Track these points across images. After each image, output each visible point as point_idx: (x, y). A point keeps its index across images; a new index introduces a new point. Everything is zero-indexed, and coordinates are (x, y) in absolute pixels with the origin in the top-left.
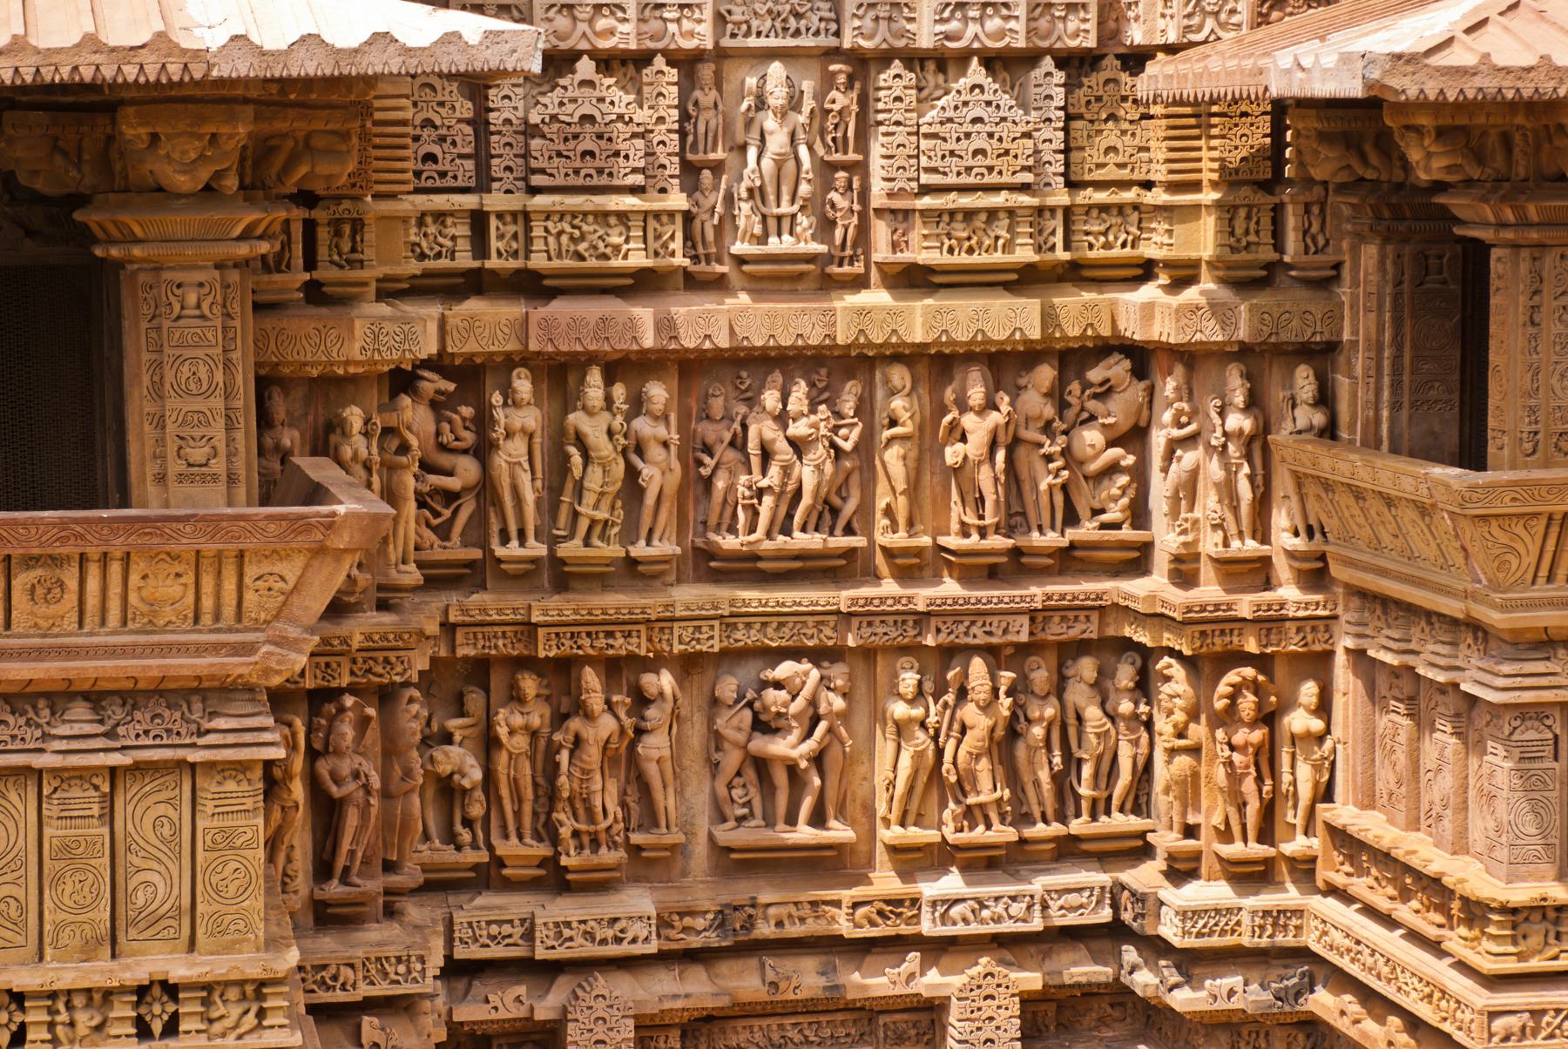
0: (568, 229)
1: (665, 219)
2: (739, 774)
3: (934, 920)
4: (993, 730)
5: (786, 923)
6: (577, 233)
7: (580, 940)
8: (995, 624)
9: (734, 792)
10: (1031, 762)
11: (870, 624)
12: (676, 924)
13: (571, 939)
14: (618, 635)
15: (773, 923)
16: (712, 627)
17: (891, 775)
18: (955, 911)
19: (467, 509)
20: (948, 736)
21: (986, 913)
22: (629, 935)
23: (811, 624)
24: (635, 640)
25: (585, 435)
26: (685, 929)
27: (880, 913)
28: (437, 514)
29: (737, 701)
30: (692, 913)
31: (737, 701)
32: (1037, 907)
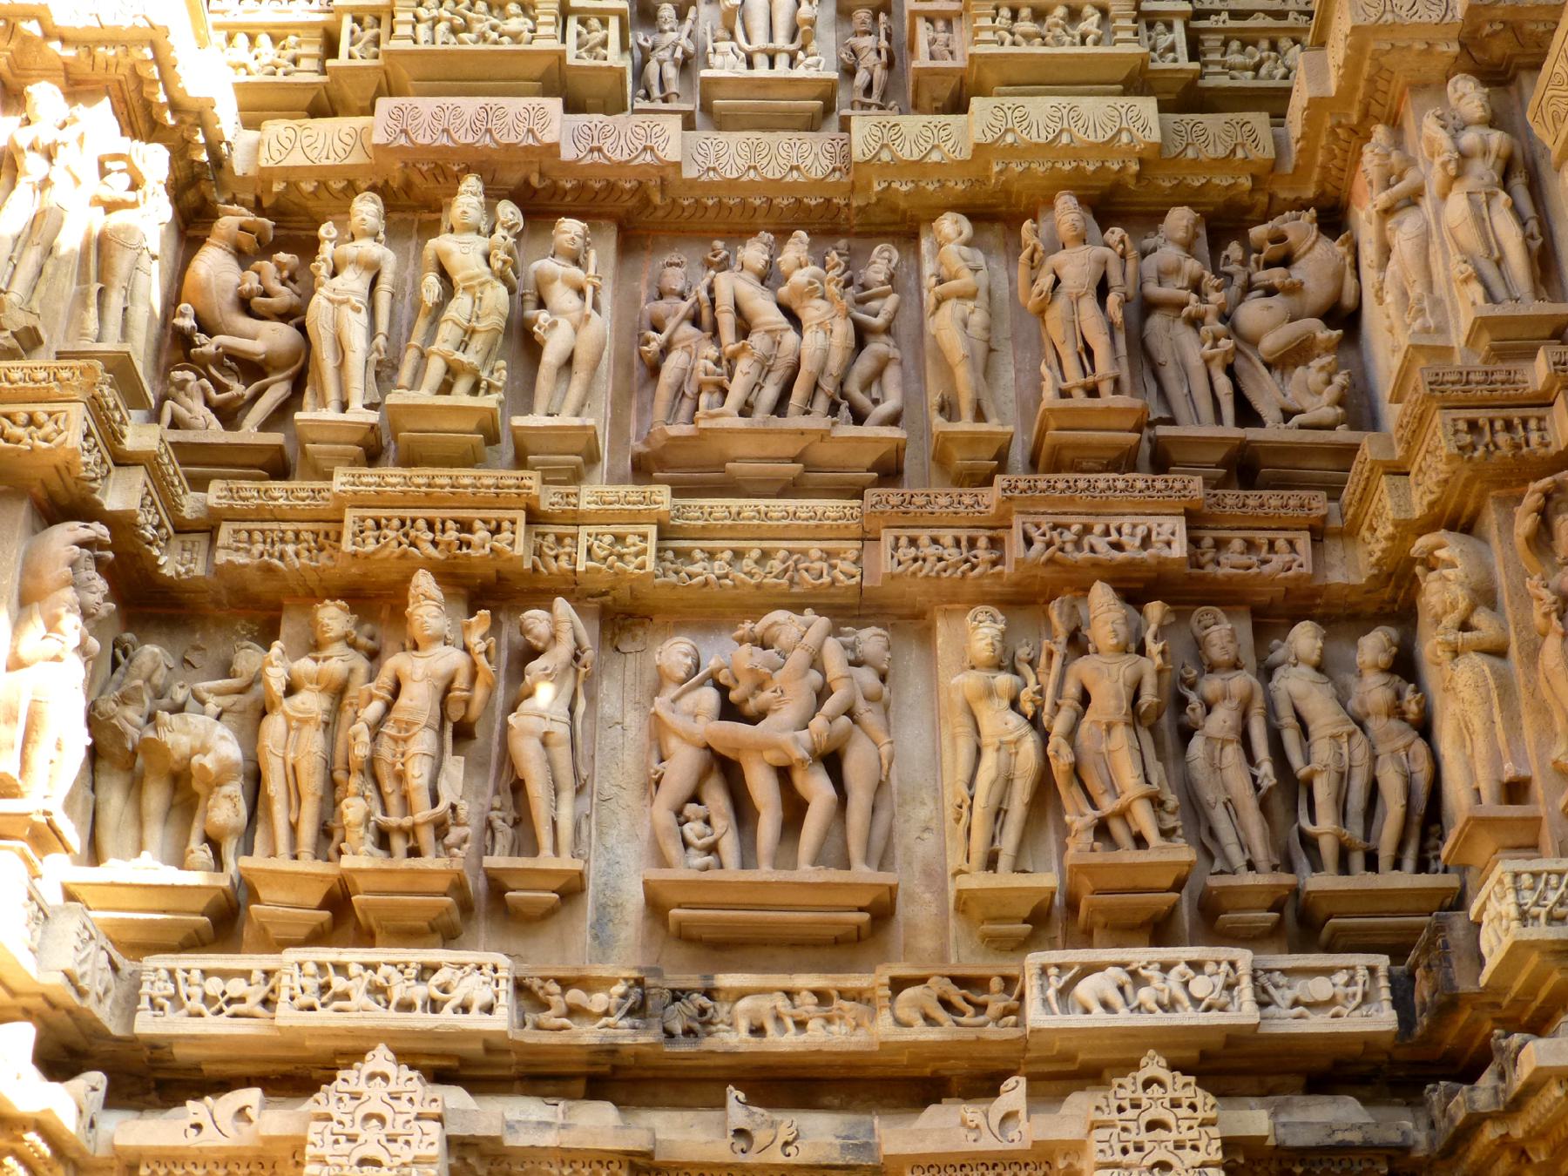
0: (447, 15)
1: (594, 23)
2: (696, 798)
3: (1045, 1001)
5: (770, 1026)
6: (459, 21)
7: (360, 998)
8: (1126, 529)
9: (686, 827)
10: (1216, 768)
11: (913, 542)
12: (554, 1000)
13: (345, 996)
14: (478, 524)
15: (743, 1025)
16: (644, 537)
18: (1086, 989)
19: (277, 391)
20: (1057, 707)
21: (1145, 994)
22: (456, 997)
23: (815, 553)
24: (506, 535)
25: (448, 254)
26: (573, 1011)
27: (946, 1004)
28: (220, 387)
29: (689, 676)
30: (585, 983)
31: (689, 676)
32: (1246, 982)
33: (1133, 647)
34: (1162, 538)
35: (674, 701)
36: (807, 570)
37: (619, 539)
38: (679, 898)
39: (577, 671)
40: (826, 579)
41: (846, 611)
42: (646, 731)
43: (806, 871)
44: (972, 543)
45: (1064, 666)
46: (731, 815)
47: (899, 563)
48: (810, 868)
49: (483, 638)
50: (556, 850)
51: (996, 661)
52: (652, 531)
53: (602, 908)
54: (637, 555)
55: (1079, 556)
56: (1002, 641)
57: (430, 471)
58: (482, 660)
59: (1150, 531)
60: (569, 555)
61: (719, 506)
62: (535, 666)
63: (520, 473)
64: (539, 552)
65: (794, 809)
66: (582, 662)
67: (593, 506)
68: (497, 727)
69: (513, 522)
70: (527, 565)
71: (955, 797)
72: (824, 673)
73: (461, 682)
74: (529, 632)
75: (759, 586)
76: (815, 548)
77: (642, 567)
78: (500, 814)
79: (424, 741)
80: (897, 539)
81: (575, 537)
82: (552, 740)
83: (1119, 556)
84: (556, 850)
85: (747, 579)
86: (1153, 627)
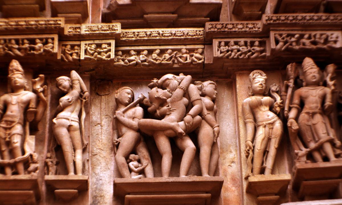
4: (323, 98)
8: (318, 36)
9: (131, 164)
11: (227, 44)
14: (38, 41)
16: (109, 45)
17: (250, 143)
20: (290, 109)
23: (184, 51)
24: (50, 45)
29: (130, 102)
31: (130, 102)
33: (321, 83)
34: (332, 39)
35: (124, 112)
36: (181, 57)
37: (99, 46)
38: (129, 190)
39: (82, 101)
40: (189, 61)
41: (199, 73)
42: (111, 127)
43: (183, 177)
44: (252, 44)
45: (293, 92)
46: (150, 159)
47: (221, 53)
48: (184, 176)
49: (42, 86)
50: (76, 172)
51: (263, 92)
52: (113, 42)
53: (95, 197)
54: (106, 52)
55: (297, 47)
56: (265, 84)
57: (16, 19)
58: (42, 95)
59: (328, 37)
60: (77, 53)
61: (142, 32)
62: (64, 99)
63: (55, 19)
64: (64, 52)
65: (177, 154)
66: (84, 97)
67: (87, 32)
68: (47, 126)
69: (53, 39)
70: (59, 58)
71: (246, 147)
72: (189, 98)
73: (33, 105)
74: (60, 85)
75: (160, 64)
76: (184, 48)
77: (109, 56)
78: (51, 160)
79: (18, 129)
80: (220, 43)
81: (79, 46)
82: (72, 128)
83: (314, 47)
84: (76, 172)
85: (155, 61)
86: (330, 75)
